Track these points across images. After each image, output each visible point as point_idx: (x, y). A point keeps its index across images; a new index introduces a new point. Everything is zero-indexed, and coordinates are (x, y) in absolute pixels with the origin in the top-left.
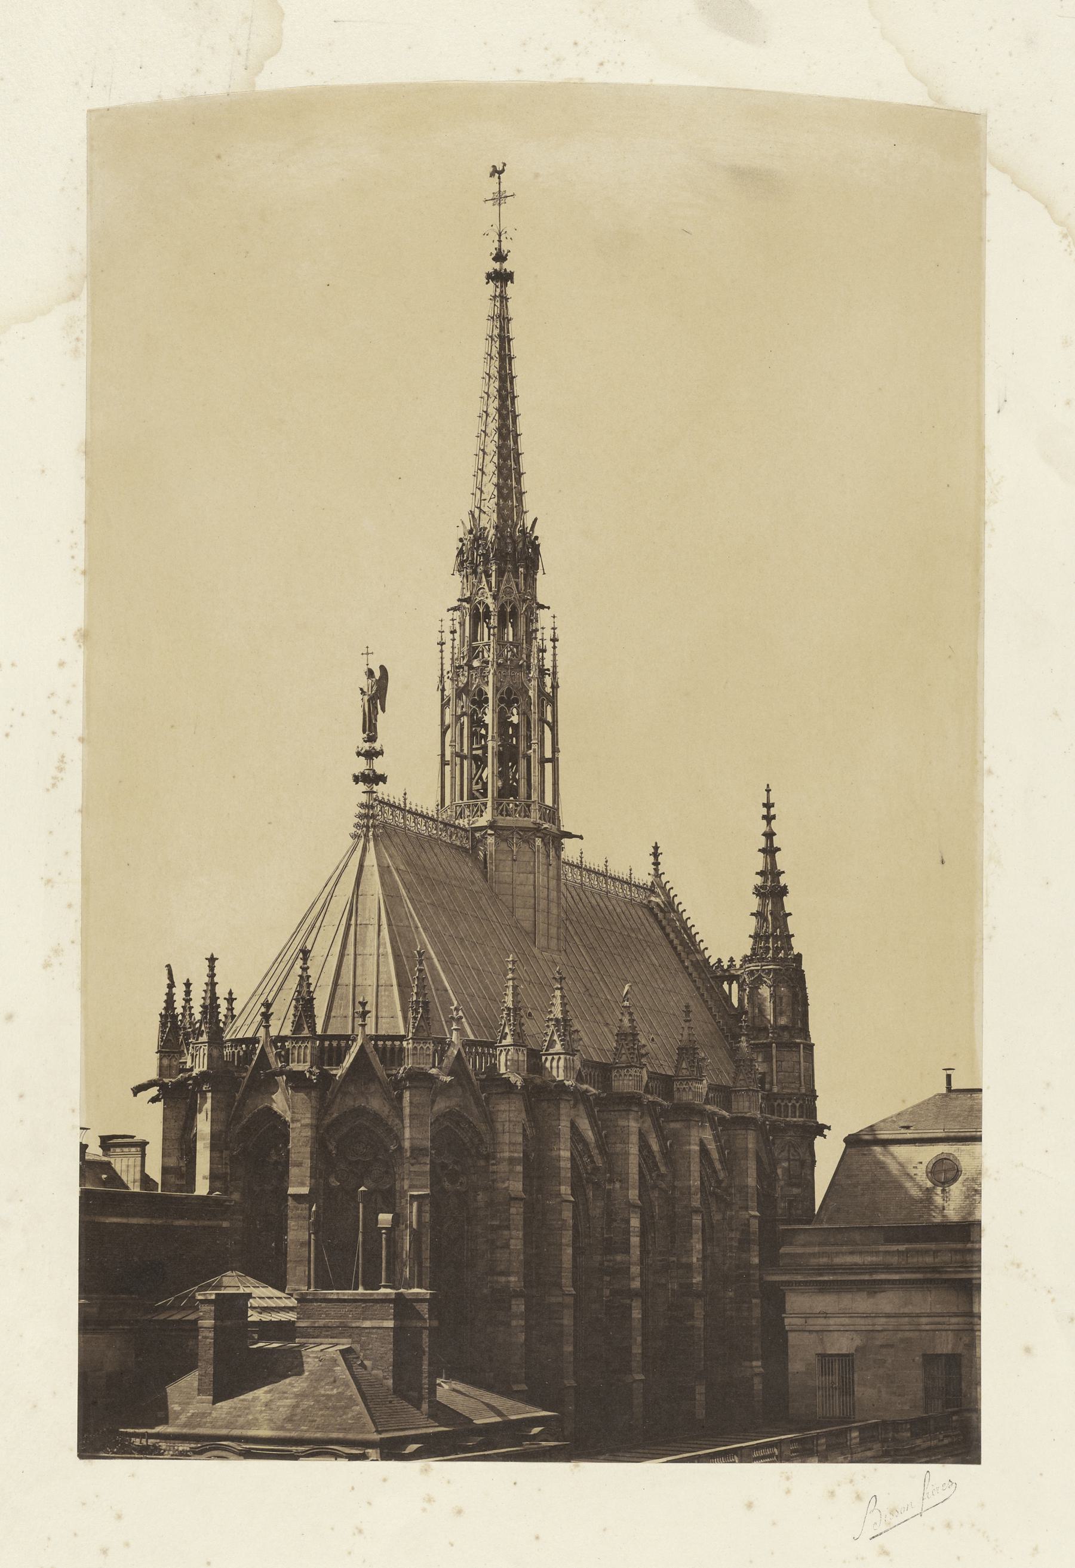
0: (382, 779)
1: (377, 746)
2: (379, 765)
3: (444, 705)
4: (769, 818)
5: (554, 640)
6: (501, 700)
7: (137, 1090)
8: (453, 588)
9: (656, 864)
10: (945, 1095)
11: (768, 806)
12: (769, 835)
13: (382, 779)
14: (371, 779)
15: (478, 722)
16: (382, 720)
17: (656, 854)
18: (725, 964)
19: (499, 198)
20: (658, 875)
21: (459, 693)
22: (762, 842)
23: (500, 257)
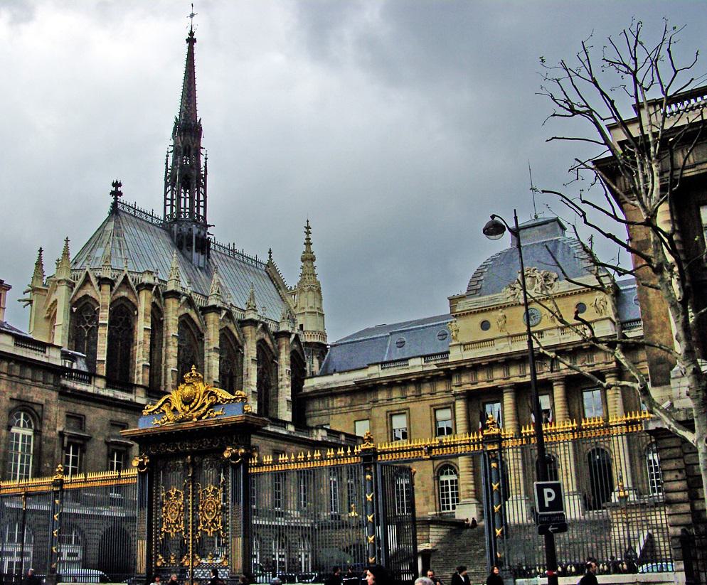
4: (308, 233)
5: (206, 159)
6: (184, 178)
9: (270, 256)
14: (116, 194)
17: (270, 252)
18: (293, 289)
19: (192, 15)
20: (271, 259)
23: (192, 34)
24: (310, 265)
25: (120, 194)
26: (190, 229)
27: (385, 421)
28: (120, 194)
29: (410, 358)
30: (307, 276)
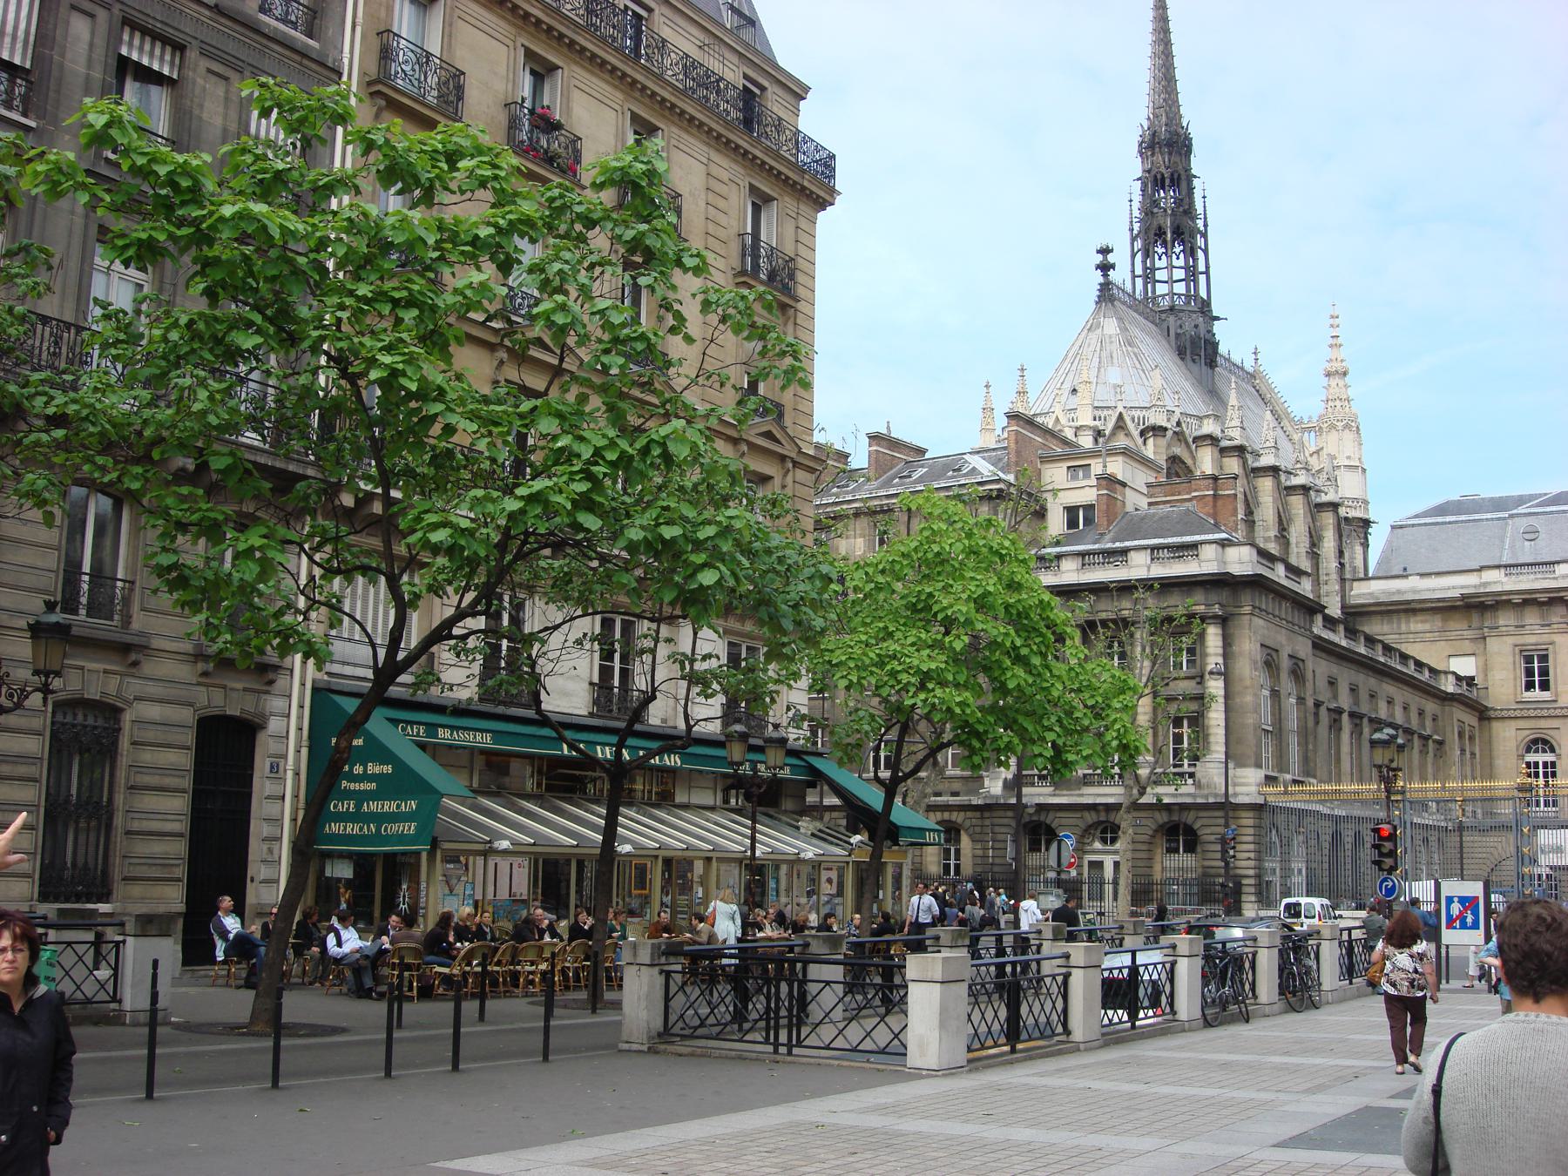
3: (1133, 239)
8: (1136, 167)
24: (1341, 383)
25: (1113, 266)
26: (1196, 326)
27: (1511, 659)
28: (1113, 266)
29: (1558, 562)
30: (1338, 403)
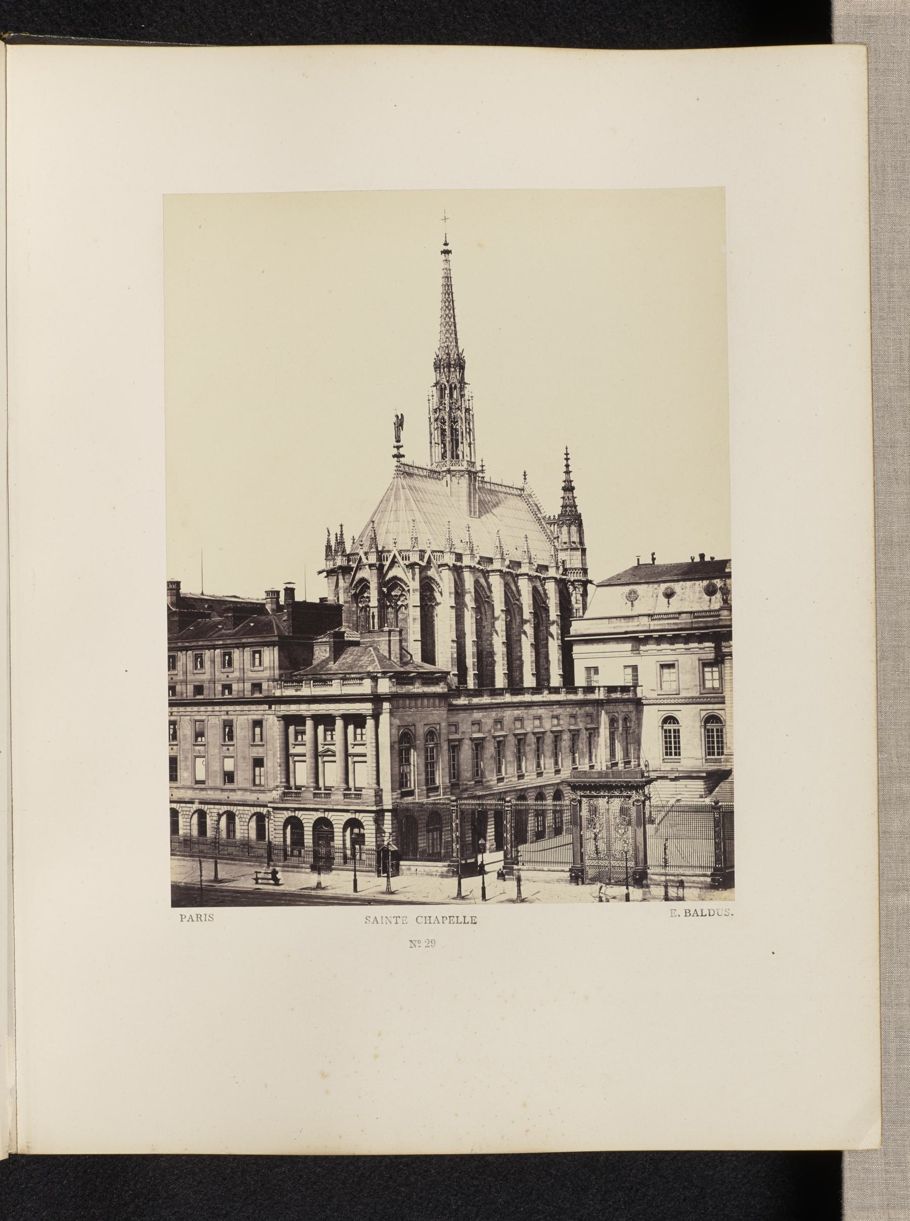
0: (403, 456)
1: (400, 444)
2: (402, 451)
4: (567, 459)
7: (320, 572)
10: (636, 567)
11: (567, 454)
12: (567, 466)
13: (403, 456)
14: (398, 456)
15: (443, 431)
16: (403, 434)
17: (525, 475)
21: (436, 420)
22: (565, 469)
